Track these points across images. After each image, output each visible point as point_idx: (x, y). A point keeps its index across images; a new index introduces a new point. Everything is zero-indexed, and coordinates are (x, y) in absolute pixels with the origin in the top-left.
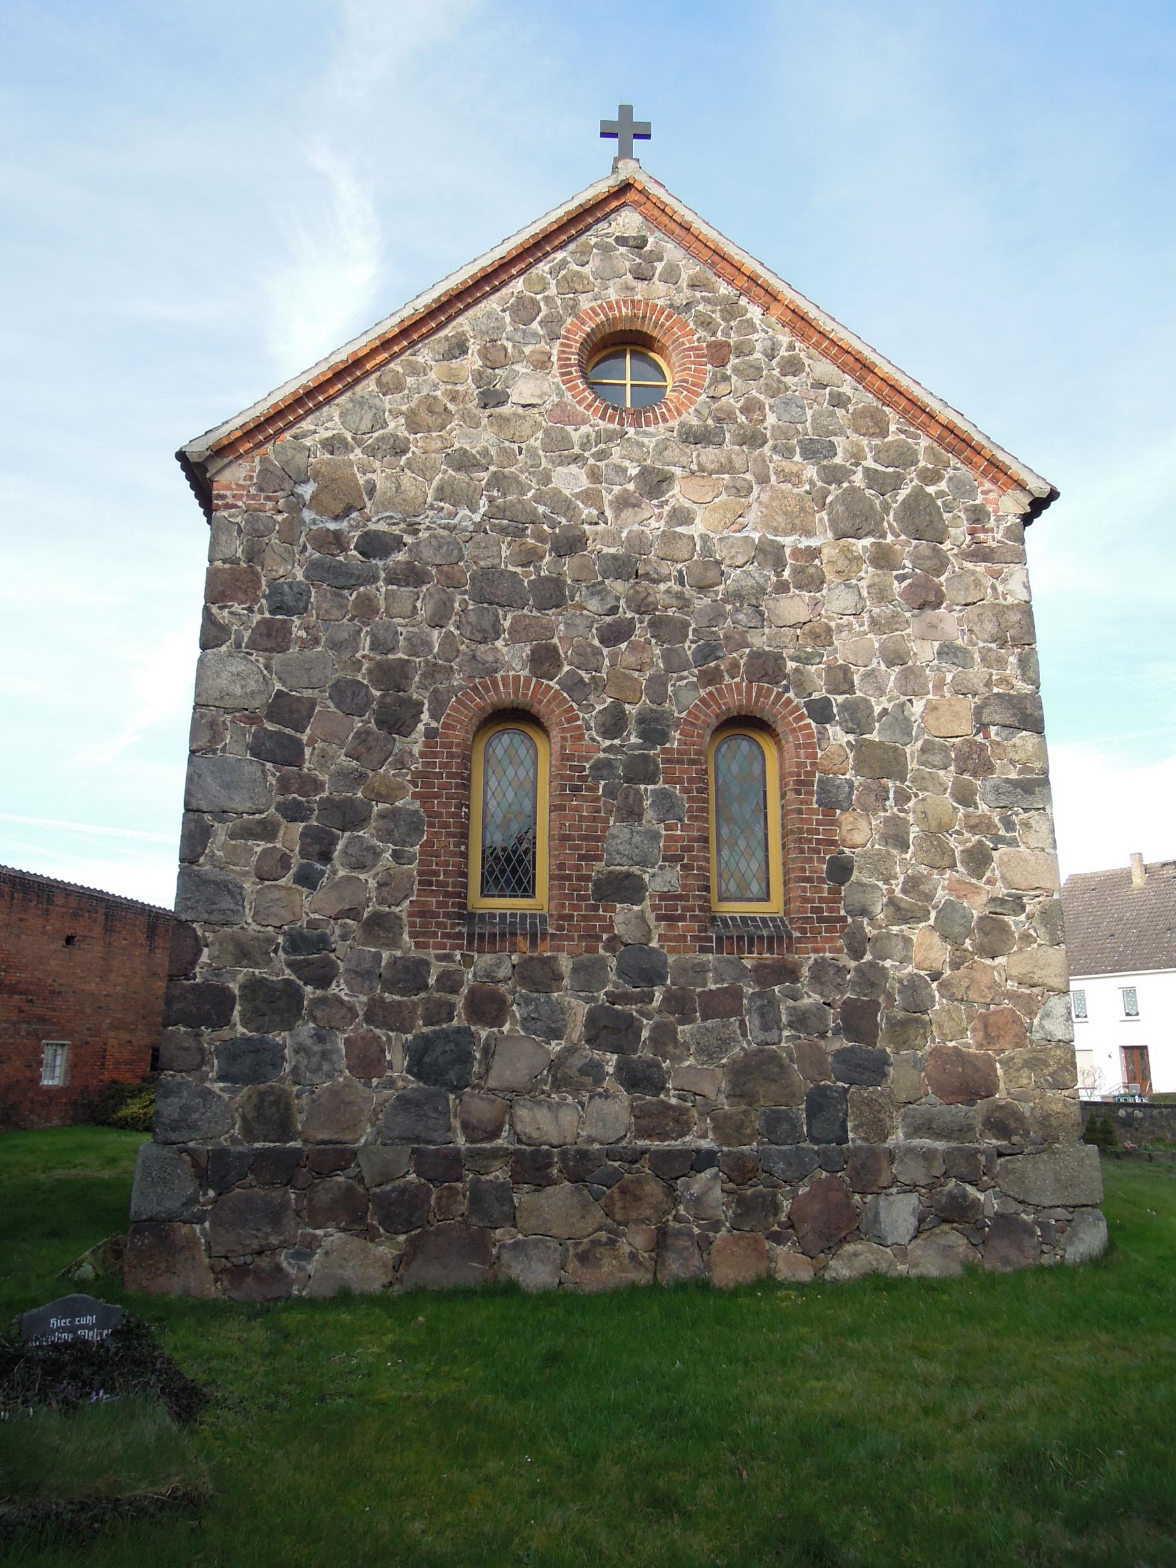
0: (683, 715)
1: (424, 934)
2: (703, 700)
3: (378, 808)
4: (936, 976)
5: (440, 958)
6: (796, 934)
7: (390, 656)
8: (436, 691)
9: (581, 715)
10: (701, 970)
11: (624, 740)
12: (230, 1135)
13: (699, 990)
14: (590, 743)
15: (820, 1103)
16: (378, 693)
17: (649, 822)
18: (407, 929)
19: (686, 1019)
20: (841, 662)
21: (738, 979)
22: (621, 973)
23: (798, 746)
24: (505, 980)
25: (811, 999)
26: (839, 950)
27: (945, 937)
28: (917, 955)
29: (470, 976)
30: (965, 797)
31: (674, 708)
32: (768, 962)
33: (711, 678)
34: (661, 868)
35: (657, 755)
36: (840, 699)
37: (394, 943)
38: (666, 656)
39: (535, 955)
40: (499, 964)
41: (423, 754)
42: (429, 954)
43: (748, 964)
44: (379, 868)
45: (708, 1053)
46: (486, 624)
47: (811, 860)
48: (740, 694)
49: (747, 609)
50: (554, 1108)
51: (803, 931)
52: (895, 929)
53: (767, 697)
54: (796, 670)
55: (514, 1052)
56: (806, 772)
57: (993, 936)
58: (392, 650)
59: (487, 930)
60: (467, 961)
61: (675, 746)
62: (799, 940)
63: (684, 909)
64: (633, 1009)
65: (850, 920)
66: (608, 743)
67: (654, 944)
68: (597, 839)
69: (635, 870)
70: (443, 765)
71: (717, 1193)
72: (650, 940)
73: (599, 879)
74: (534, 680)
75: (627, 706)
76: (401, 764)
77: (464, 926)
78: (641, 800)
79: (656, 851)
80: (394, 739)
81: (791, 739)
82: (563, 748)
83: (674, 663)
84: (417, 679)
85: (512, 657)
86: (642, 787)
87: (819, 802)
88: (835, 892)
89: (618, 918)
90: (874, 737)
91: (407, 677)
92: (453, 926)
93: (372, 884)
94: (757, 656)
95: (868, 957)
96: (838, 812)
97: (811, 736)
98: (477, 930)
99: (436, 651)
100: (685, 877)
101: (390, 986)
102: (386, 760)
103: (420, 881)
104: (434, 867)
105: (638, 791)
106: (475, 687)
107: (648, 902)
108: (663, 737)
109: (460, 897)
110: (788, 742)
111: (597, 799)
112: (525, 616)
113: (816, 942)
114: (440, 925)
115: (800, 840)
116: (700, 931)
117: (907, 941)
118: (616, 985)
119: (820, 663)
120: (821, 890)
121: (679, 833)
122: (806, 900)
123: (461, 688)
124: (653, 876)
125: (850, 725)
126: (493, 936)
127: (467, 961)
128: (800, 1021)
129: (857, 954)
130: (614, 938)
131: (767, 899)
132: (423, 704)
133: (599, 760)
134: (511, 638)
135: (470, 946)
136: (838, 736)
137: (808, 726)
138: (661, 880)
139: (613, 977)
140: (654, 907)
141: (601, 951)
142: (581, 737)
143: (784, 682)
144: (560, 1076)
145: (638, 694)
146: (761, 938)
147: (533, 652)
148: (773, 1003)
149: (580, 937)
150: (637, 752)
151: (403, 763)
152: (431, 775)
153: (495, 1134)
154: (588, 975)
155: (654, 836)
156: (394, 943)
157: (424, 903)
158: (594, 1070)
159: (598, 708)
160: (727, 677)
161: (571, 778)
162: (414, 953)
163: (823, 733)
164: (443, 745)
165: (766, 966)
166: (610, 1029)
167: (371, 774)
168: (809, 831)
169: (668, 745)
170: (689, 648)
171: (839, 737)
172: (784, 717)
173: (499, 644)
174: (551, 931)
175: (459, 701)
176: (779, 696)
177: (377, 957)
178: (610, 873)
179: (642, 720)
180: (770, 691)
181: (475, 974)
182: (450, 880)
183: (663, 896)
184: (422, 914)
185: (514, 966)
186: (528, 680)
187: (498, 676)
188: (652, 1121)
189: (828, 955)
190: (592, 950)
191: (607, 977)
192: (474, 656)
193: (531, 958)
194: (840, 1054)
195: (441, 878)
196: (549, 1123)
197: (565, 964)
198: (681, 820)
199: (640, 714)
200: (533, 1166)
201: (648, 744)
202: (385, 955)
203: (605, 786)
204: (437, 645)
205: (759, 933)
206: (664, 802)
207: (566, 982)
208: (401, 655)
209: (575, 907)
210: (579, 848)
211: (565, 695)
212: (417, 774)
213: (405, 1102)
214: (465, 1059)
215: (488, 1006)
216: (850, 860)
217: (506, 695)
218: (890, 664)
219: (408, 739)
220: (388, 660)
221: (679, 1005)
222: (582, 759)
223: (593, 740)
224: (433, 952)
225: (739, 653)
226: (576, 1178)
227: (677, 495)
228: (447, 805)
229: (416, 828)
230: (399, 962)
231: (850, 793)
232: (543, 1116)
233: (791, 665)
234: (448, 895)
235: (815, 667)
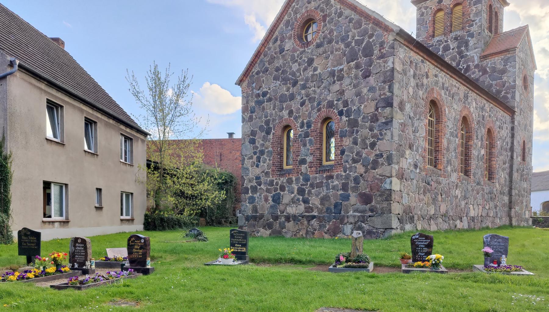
4: (361, 175)
12: (250, 213)
15: (336, 205)
19: (313, 189)
22: (303, 180)
25: (336, 183)
26: (341, 171)
27: (364, 166)
28: (358, 171)
30: (371, 129)
33: (319, 110)
36: (345, 109)
38: (311, 107)
40: (284, 180)
43: (325, 176)
45: (317, 196)
49: (327, 90)
50: (292, 207)
52: (353, 165)
54: (337, 104)
55: (287, 198)
57: (375, 165)
64: (304, 187)
71: (315, 224)
85: (285, 113)
90: (352, 117)
94: (329, 102)
95: (348, 172)
101: (269, 185)
117: (356, 167)
128: (334, 188)
129: (345, 172)
136: (344, 118)
138: (309, 159)
144: (294, 201)
148: (329, 184)
153: (283, 213)
154: (297, 180)
155: (308, 149)
158: (298, 199)
166: (301, 191)
170: (315, 104)
183: (310, 162)
188: (309, 209)
190: (298, 175)
194: (341, 195)
196: (292, 210)
197: (294, 179)
200: (288, 219)
213: (271, 207)
214: (279, 198)
215: (282, 188)
216: (345, 150)
218: (357, 96)
221: (312, 186)
226: (294, 220)
227: (315, 64)
232: (290, 208)
233: (335, 102)
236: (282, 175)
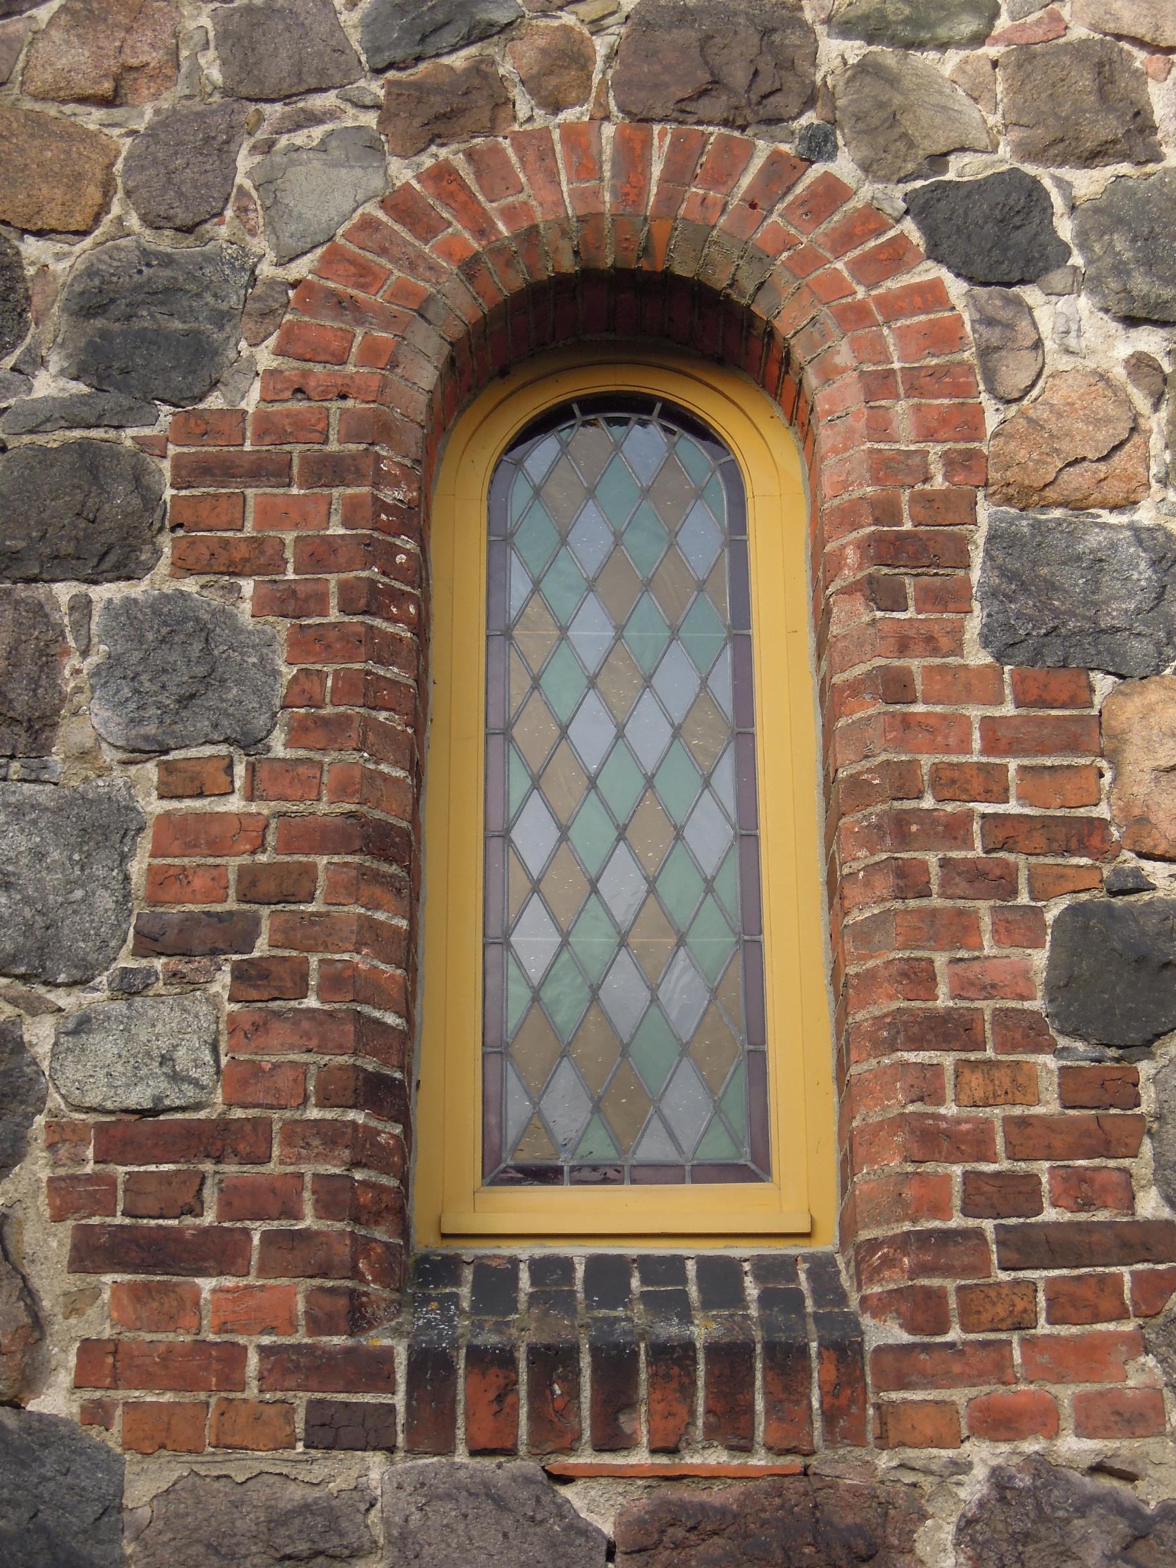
0: (300, 269)
2: (401, 205)
6: (884, 1332)
17: (84, 755)
20: (1079, 32)
23: (879, 385)
31: (259, 244)
32: (717, 1496)
34: (129, 987)
35: (156, 447)
36: (1089, 182)
43: (599, 1508)
47: (961, 929)
48: (587, 167)
51: (925, 1312)
53: (723, 177)
54: (865, 69)
56: (927, 500)
61: (251, 402)
62: (900, 1366)
63: (239, 1201)
67: (56, 1400)
72: (31, 1378)
78: (48, 659)
79: (105, 901)
81: (844, 355)
86: (64, 592)
96: (1103, 683)
97: (945, 336)
105: (39, 611)
108: (199, 364)
110: (829, 375)
113: (1000, 1370)
115: (899, 828)
116: (317, 1325)
119: (978, 40)
120: (1022, 1085)
121: (235, 804)
122: (932, 1140)
124: (83, 1025)
125: (1140, 283)
131: (752, 1166)
137: (933, 295)
140: (67, 1196)
143: (809, 118)
145: (93, 194)
146: (674, 1358)
150: (54, 439)
155: (103, 828)
160: (523, 105)
163: (1005, 334)
165: (699, 1523)
168: (948, 783)
169: (215, 401)
171: (1091, 337)
172: (808, 261)
176: (780, 173)
179: (93, 301)
180: (732, 159)
183: (130, 1132)
189: (1073, 1447)
198: (251, 743)
199: (90, 272)
201: (112, 400)
205: (670, 1330)
206: (177, 671)
233: (836, 53)
235: (954, 57)
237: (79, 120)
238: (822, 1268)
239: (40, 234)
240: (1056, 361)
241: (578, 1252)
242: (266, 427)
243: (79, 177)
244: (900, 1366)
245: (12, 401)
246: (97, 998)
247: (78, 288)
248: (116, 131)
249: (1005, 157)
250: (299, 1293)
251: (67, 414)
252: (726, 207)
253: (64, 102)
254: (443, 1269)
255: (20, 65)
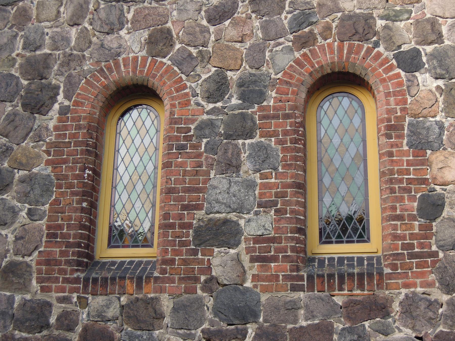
0: (279, 76)
1: (48, 280)
2: (297, 62)
3: (19, 174)
5: (61, 300)
6: (387, 271)
7: (38, 53)
8: (70, 76)
9: (188, 84)
10: (293, 307)
11: (226, 102)
13: (290, 326)
14: (195, 107)
16: (25, 83)
17: (246, 172)
18: (35, 275)
20: (428, 16)
21: (329, 316)
22: (217, 311)
23: (388, 94)
24: (114, 319)
26: (431, 285)
29: (85, 316)
31: (271, 71)
32: (359, 298)
33: (304, 42)
34: (257, 214)
35: (255, 113)
36: (429, 49)
37: (24, 287)
38: (264, 28)
39: (140, 296)
41: (56, 128)
42: (51, 297)
43: (339, 300)
44: (16, 225)
46: (114, 18)
47: (401, 199)
48: (332, 52)
51: (394, 267)
53: (358, 53)
54: (386, 27)
56: (396, 117)
58: (38, 48)
59: (105, 274)
60: (83, 303)
61: (272, 103)
62: (390, 276)
63: (278, 250)
65: (441, 255)
66: (211, 106)
67: (248, 284)
68: (199, 190)
69: (233, 216)
70: (73, 136)
72: (244, 281)
73: (200, 227)
74: (150, 59)
75: (229, 74)
76: (39, 138)
77: (82, 271)
78: (239, 154)
79: (252, 198)
80: (35, 117)
81: (381, 89)
82: (172, 113)
83: (271, 34)
84: (56, 68)
86: (240, 141)
87: (411, 145)
88: (427, 228)
89: (215, 261)
91: (48, 67)
92: (72, 272)
93: (11, 238)
94: (350, 18)
96: (429, 152)
97: (400, 84)
98: (94, 275)
99: (73, 44)
100: (278, 221)
102: (27, 135)
103: (48, 234)
104: (60, 222)
105: (236, 146)
106: (102, 70)
107: (243, 245)
108: (261, 96)
109: (80, 246)
110: (379, 92)
111: (199, 155)
112: (145, 8)
113: (407, 277)
114: (61, 271)
115: (391, 181)
116: (291, 271)
118: (212, 323)
119: (408, 19)
120: (412, 227)
121: (273, 180)
122: (396, 237)
123: (90, 71)
124: (249, 221)
125: (438, 71)
126: (105, 280)
127: (83, 303)
130: (212, 279)
132: (59, 87)
133: (202, 122)
134: (133, 27)
135: (85, 291)
138: (256, 225)
139: (209, 315)
140: (249, 251)
141: (199, 292)
142: (188, 103)
143: (375, 39)
145: (239, 62)
146: (351, 275)
147: (150, 36)
149: (180, 279)
150: (236, 112)
151: (40, 137)
152: (62, 145)
155: (251, 185)
156: (24, 287)
157: (49, 253)
159: (204, 77)
160: (320, 39)
161: (178, 139)
162: (40, 296)
163: (412, 82)
164: (73, 119)
165: (356, 303)
167: (15, 147)
168: (400, 172)
169: (265, 103)
170: (286, 18)
171: (429, 82)
172: (374, 70)
173: (123, 33)
174: (156, 274)
175: (88, 82)
176: (369, 51)
177: (11, 300)
178: (210, 220)
179: (241, 84)
180: (360, 48)
181: (88, 314)
182: (72, 232)
183: (258, 239)
184: (48, 263)
185: (122, 307)
186: (144, 59)
187: (120, 59)
189: (419, 290)
191: (203, 315)
192: (102, 45)
193: (137, 299)
195: (65, 231)
197: (166, 303)
198: (275, 169)
199: (240, 78)
201: (247, 104)
202: (18, 298)
203: (207, 143)
204: (74, 39)
205: (351, 271)
206: (262, 155)
207: (167, 320)
208: (47, 51)
209: (177, 253)
210: (182, 199)
211: (176, 68)
212: (51, 145)
217: (126, 74)
219: (46, 117)
220: (35, 56)
222: (188, 121)
223: (198, 104)
224: (55, 295)
225: (332, 17)
228: (73, 169)
229: (47, 191)
230: (29, 304)
231: (441, 134)
233: (380, 23)
234: (69, 245)
235: (403, 23)
236: (100, 285)
237: (235, 46)
238: (378, 258)
239: (230, 70)
240: (422, 88)
241: (336, 256)
242: (275, 108)
243: (236, 58)
244: (390, 276)
245: (228, 105)
246: (251, 216)
247: (238, 82)
248: (243, 48)
249: (413, 45)
250: (288, 265)
251: (238, 107)
252: (359, 63)
253: (232, 42)
254: (312, 260)
255: (223, 35)
